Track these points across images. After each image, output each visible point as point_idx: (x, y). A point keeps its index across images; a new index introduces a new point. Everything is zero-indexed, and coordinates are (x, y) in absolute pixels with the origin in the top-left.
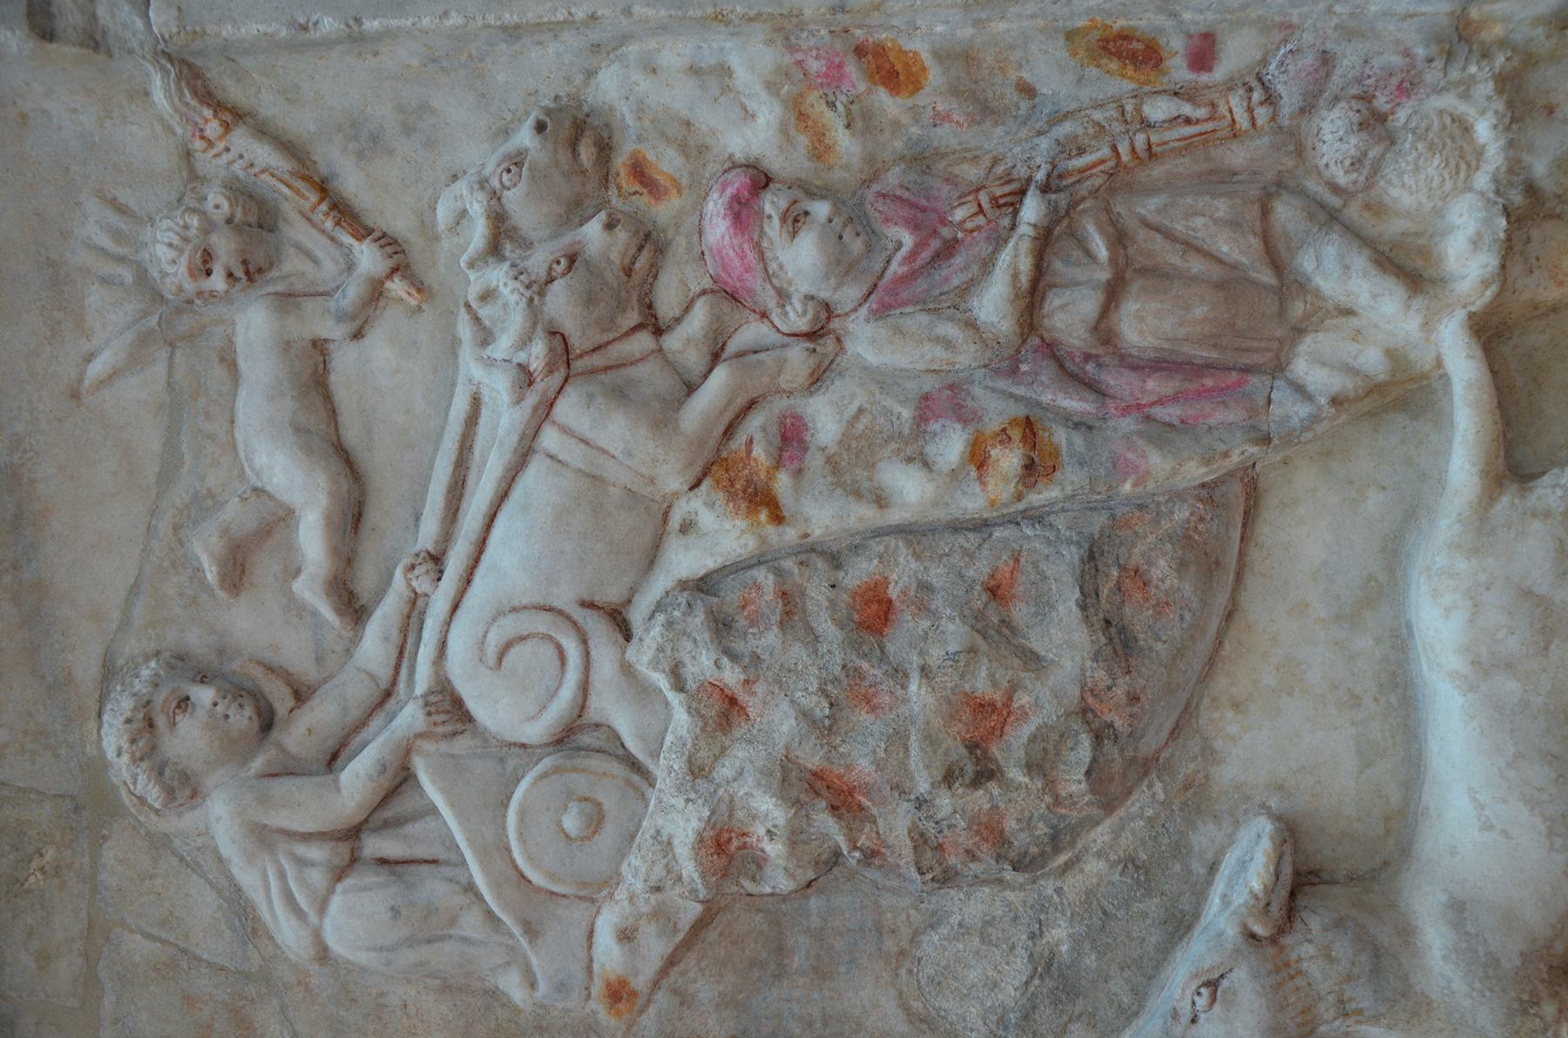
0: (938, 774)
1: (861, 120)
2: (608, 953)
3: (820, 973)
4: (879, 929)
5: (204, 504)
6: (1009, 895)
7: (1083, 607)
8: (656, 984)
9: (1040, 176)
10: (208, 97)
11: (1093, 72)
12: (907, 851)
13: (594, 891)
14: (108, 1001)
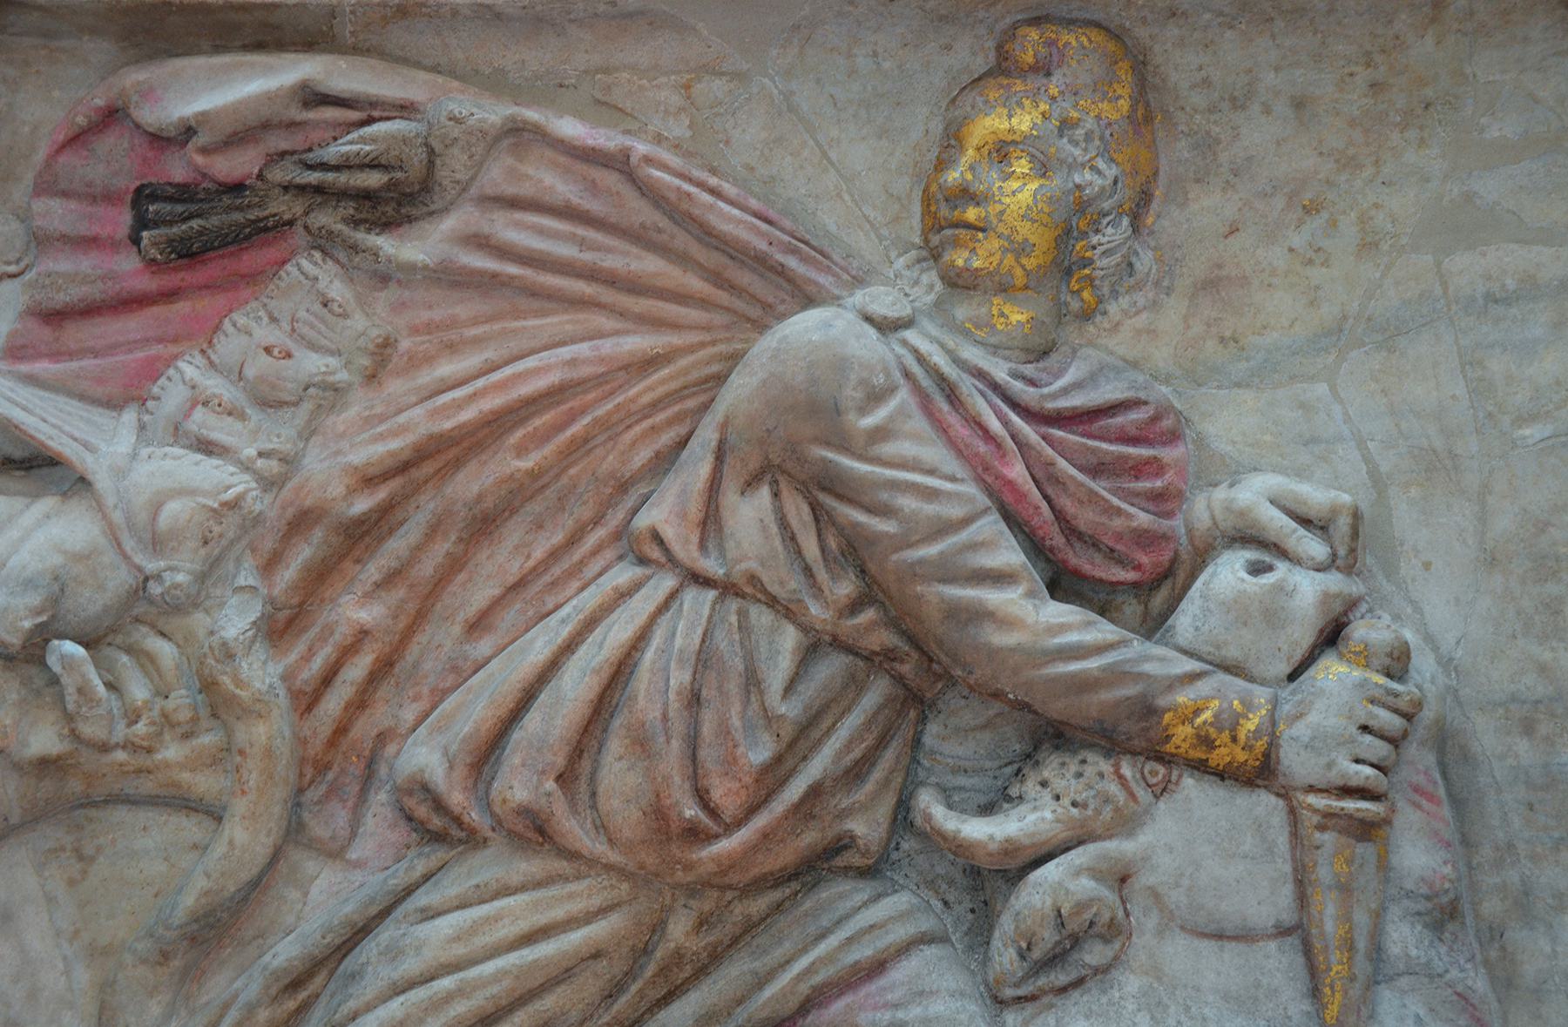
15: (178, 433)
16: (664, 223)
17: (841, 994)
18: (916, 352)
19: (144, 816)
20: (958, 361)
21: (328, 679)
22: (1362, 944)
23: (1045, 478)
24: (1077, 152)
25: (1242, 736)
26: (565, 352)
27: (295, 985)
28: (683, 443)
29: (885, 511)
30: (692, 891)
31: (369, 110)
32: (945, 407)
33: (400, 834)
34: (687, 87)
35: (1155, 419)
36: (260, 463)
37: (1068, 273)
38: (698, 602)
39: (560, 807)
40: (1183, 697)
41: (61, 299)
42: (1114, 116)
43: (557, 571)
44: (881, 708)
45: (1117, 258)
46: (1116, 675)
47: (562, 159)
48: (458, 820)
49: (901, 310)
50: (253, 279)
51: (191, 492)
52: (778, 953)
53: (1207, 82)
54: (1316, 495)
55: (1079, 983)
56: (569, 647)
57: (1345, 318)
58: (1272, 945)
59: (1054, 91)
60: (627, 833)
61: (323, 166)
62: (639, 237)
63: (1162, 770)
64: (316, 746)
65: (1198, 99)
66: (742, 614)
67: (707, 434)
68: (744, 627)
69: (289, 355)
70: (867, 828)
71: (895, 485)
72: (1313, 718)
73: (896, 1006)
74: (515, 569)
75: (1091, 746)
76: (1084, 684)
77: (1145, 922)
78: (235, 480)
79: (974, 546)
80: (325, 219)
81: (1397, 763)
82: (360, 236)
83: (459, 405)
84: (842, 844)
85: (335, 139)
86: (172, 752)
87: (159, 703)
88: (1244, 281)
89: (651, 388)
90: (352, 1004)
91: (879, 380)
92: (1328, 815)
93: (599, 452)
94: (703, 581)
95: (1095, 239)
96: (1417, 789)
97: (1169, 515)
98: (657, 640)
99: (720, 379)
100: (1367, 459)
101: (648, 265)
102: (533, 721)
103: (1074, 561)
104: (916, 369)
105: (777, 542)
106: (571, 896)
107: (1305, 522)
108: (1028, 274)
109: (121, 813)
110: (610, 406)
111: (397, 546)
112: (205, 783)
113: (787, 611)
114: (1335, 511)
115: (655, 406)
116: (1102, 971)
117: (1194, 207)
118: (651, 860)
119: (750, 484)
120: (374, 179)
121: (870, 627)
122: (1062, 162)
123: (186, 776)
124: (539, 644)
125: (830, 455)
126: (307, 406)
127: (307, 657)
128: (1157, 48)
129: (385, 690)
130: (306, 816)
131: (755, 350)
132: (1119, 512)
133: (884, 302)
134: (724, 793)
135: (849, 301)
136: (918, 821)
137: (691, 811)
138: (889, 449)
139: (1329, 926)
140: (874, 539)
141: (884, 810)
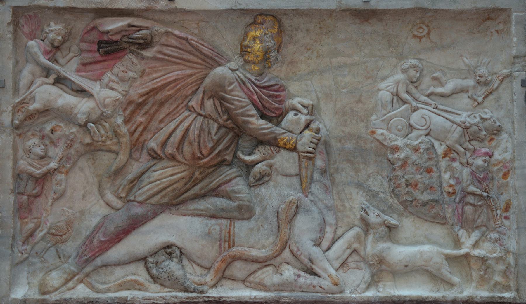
0: (407, 179)
1: (499, 170)
2: (380, 131)
3: (376, 161)
4: (382, 170)
5: (444, 74)
6: (387, 189)
7: (430, 200)
8: (374, 138)
9: (490, 195)
10: (505, 77)
11: (504, 203)
12: (395, 174)
13: (389, 129)
14: (373, 59)
15: (107, 86)
16: (194, 50)
17: (224, 185)
18: (238, 75)
19: (104, 153)
20: (245, 77)
21: (135, 130)
22: (309, 177)
23: (260, 98)
24: (268, 39)
25: (291, 143)
26: (176, 73)
27: (132, 182)
28: (198, 89)
29: (232, 104)
30: (199, 168)
31: (141, 28)
32: (243, 86)
33: (148, 157)
34: (198, 24)
35: (280, 87)
36: (122, 92)
37: (266, 60)
38: (200, 119)
39: (177, 154)
40: (282, 137)
41: (86, 61)
42: (274, 32)
43: (175, 112)
44: (231, 137)
45: (275, 58)
46: (271, 133)
47: (175, 38)
48: (159, 155)
49: (236, 67)
50: (119, 58)
51: (111, 97)
52: (214, 178)
53: (291, 26)
54: (306, 102)
55: (263, 183)
56: (178, 126)
57: (314, 69)
58: (295, 177)
59: (264, 28)
60: (188, 158)
61: (133, 39)
62: (190, 53)
63: (278, 149)
64: (134, 142)
65: (290, 29)
66: (208, 121)
67: (201, 89)
68: (208, 124)
69: (126, 72)
70: (229, 158)
72: (303, 140)
73: (233, 187)
74: (168, 112)
75: (267, 144)
76: (265, 134)
77: (274, 173)
78: (118, 95)
79: (247, 111)
80: (133, 48)
81: (317, 148)
82: (139, 51)
83: (157, 82)
84: (225, 160)
85: (134, 33)
86: (109, 142)
87: (106, 134)
89: (191, 80)
90: (142, 185)
91: (232, 81)
92: (304, 156)
93: (182, 91)
94: (201, 115)
95: (271, 55)
96: (320, 152)
97: (282, 104)
98: (193, 125)
99: (204, 78)
100: (317, 95)
101: (191, 57)
102: (172, 139)
103: (265, 112)
104: (238, 79)
105: (214, 109)
106: (179, 168)
107: (304, 106)
108: (258, 61)
109: (100, 153)
110: (184, 83)
111: (147, 107)
112: (114, 148)
113: (216, 121)
114: (309, 105)
115: (192, 83)
116: (267, 181)
117: (289, 48)
118: (192, 163)
119: (209, 98)
120: (141, 41)
121: (229, 124)
122: (265, 41)
123: (111, 147)
124: (172, 125)
125: (223, 94)
126: (130, 82)
127: (132, 127)
128: (283, 19)
129: (145, 133)
130: (132, 154)
131: (210, 74)
133: (233, 65)
134: (204, 152)
135: (227, 65)
136: (238, 156)
137: (199, 155)
138: (233, 93)
139: (304, 174)
140: (230, 109)
141: (232, 155)
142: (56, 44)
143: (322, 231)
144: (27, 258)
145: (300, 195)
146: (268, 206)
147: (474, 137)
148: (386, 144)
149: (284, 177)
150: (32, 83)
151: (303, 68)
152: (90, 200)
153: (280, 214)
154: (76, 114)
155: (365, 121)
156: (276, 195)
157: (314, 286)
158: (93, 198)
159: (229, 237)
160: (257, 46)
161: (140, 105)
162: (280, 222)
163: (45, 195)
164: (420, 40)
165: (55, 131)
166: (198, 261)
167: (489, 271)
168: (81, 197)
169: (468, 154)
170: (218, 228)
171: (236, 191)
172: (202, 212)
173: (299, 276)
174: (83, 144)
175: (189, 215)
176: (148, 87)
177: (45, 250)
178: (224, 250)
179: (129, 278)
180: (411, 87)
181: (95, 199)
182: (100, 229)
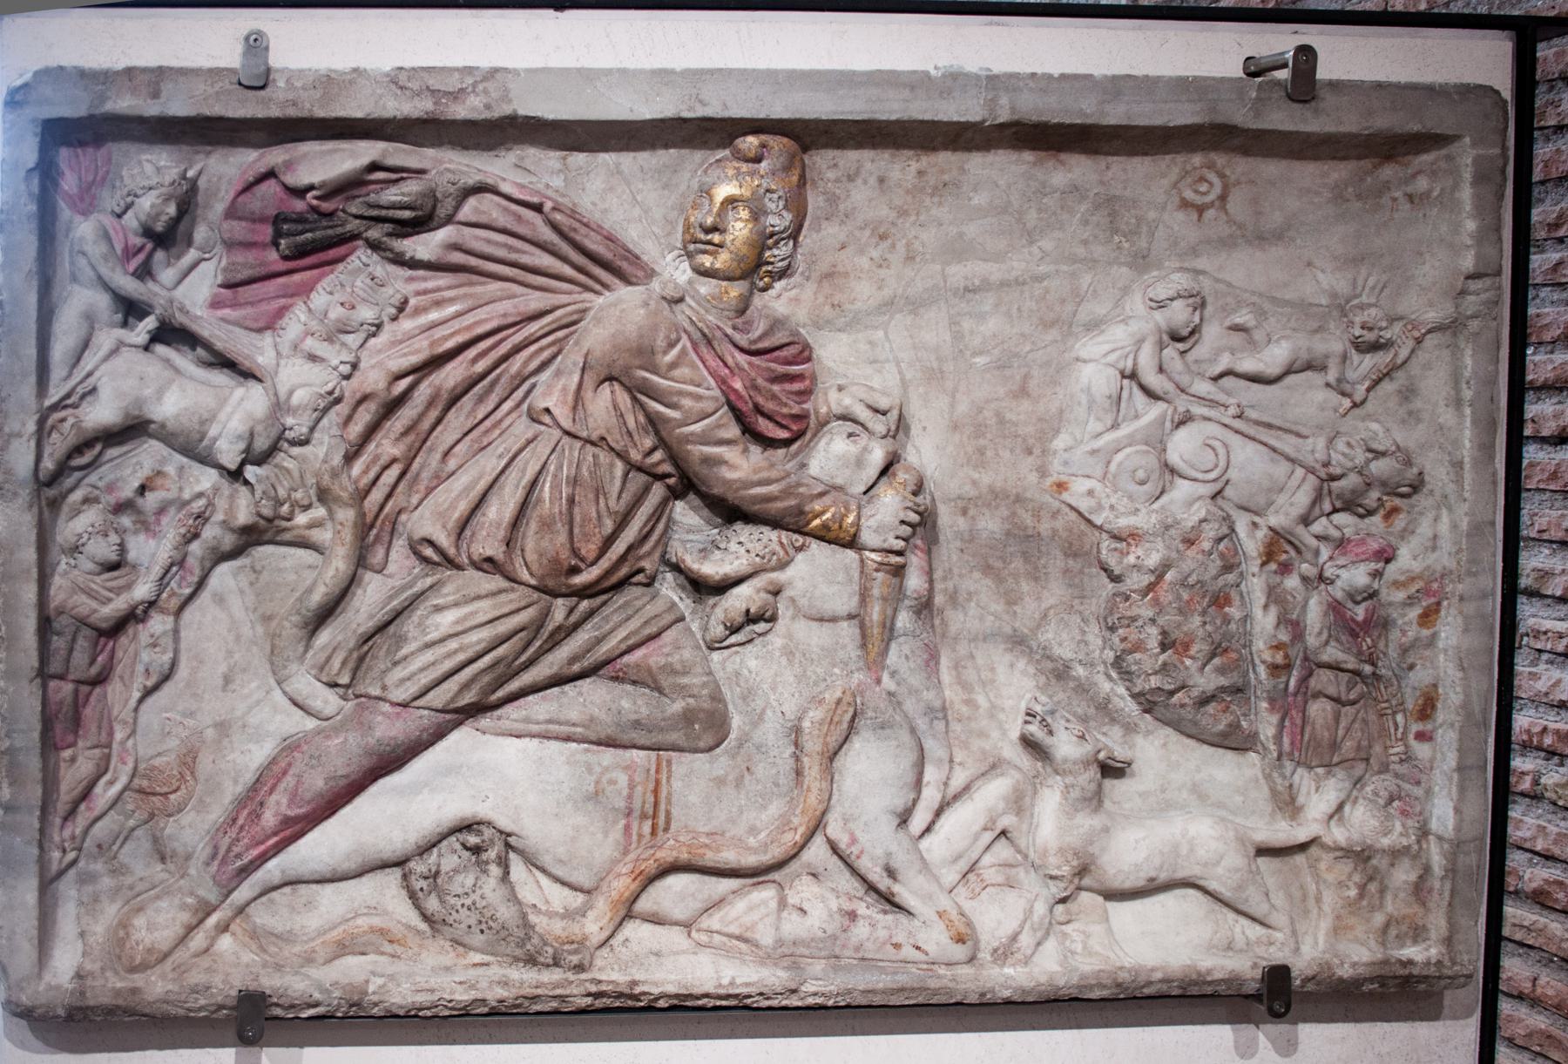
1: (1410, 601)
5: (1261, 314)
10: (1429, 332)
11: (1418, 693)
14: (1065, 268)
38: (573, 449)
41: (240, 277)
43: (488, 423)
58: (845, 624)
71: (681, 393)
80: (374, 233)
83: (446, 338)
88: (846, 275)
100: (900, 373)
117: (824, 233)
120: (407, 214)
125: (647, 375)
132: (786, 405)
138: (677, 373)
140: (667, 420)
142: (159, 227)
143: (918, 784)
144: (74, 862)
145: (858, 677)
146: (769, 713)
147: (1349, 505)
148: (1098, 521)
149: (815, 624)
150: (86, 345)
151: (863, 293)
152: (246, 691)
153: (806, 738)
154: (215, 440)
155: (1037, 451)
156: (792, 679)
157: (897, 946)
158: (254, 685)
159: (656, 804)
160: (739, 229)
161: (393, 406)
162: (806, 760)
163: (121, 678)
164: (1200, 216)
165: (152, 489)
166: (559, 872)
167: (1373, 887)
168: (220, 682)
169: (1325, 553)
170: (623, 779)
171: (678, 667)
172: (573, 729)
173: (852, 916)
174: (233, 530)
175: (533, 736)
176: (417, 351)
177: (121, 838)
178: (639, 841)
179: (363, 922)
180: (1170, 352)
181: (259, 687)
182: (279, 780)
